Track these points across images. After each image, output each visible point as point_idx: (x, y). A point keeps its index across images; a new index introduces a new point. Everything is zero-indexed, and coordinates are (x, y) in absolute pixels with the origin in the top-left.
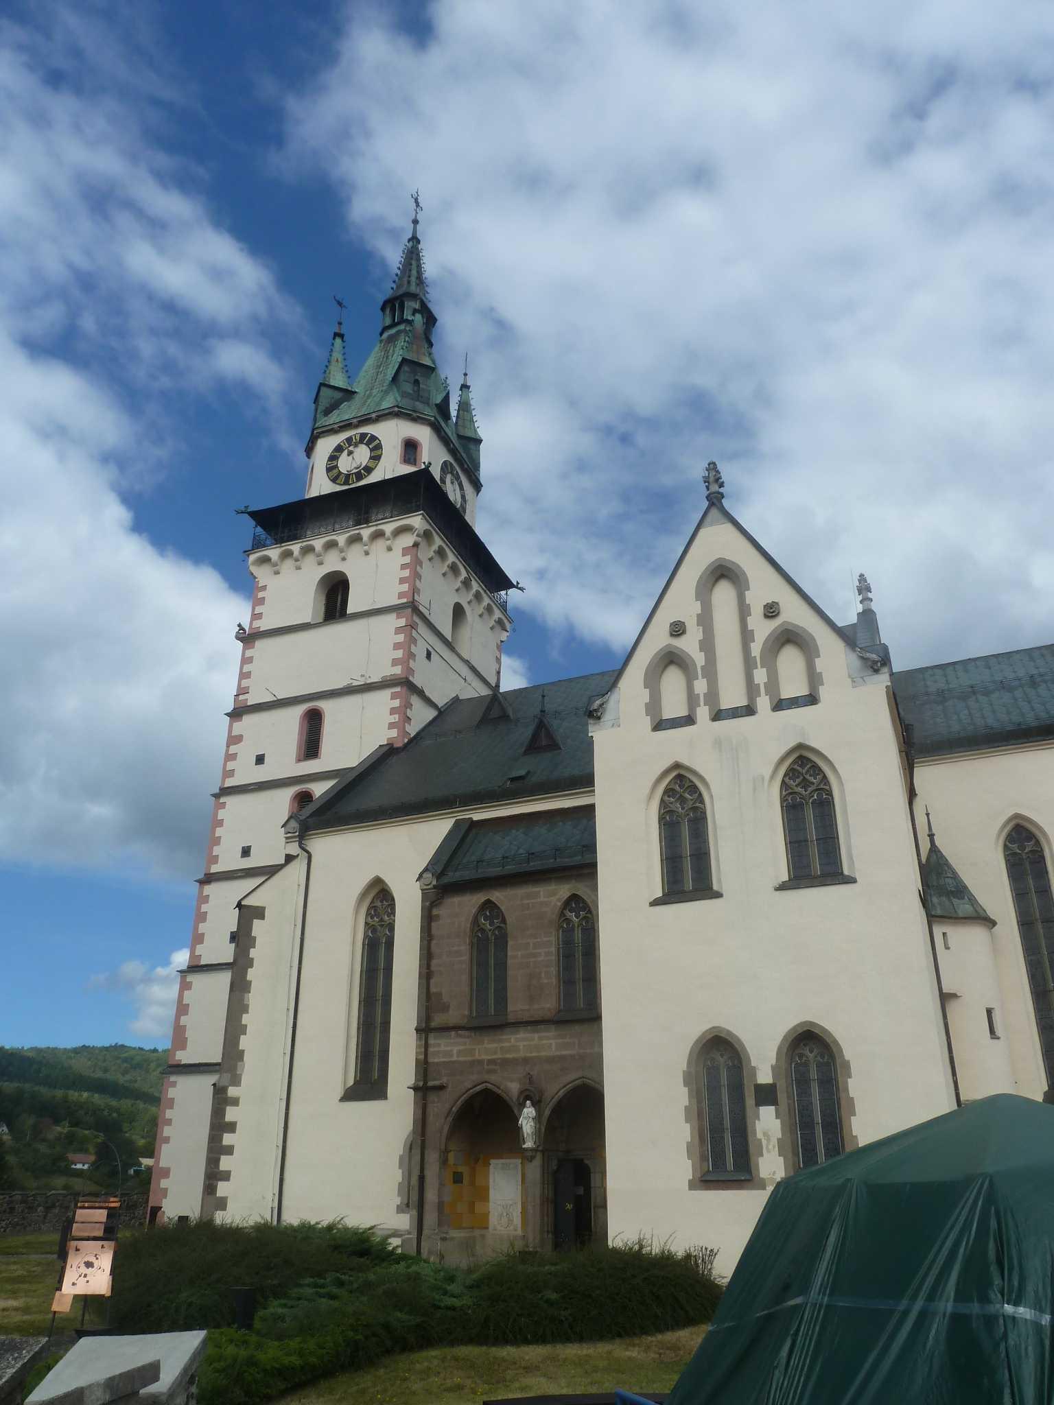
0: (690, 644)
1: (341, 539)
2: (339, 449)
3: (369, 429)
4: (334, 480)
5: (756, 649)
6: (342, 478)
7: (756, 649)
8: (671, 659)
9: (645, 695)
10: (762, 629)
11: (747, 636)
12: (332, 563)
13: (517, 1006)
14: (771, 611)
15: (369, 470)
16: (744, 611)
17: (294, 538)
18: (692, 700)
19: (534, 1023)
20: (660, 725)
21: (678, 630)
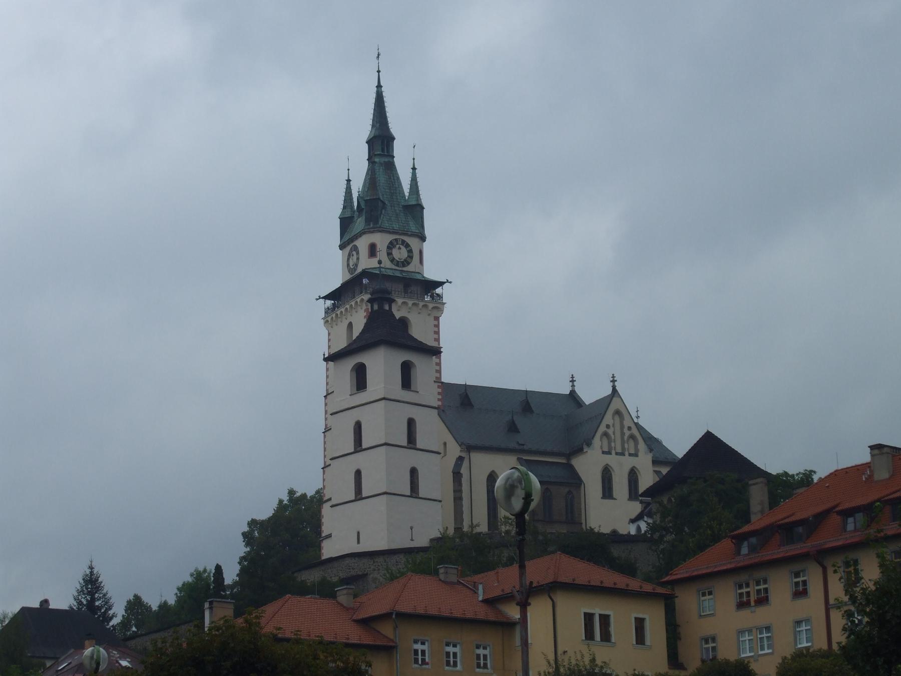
0: (610, 431)
1: (410, 303)
2: (391, 243)
5: (626, 438)
7: (626, 438)
8: (605, 434)
9: (600, 443)
10: (627, 433)
11: (623, 434)
14: (629, 428)
15: (409, 264)
20: (603, 453)
21: (608, 426)
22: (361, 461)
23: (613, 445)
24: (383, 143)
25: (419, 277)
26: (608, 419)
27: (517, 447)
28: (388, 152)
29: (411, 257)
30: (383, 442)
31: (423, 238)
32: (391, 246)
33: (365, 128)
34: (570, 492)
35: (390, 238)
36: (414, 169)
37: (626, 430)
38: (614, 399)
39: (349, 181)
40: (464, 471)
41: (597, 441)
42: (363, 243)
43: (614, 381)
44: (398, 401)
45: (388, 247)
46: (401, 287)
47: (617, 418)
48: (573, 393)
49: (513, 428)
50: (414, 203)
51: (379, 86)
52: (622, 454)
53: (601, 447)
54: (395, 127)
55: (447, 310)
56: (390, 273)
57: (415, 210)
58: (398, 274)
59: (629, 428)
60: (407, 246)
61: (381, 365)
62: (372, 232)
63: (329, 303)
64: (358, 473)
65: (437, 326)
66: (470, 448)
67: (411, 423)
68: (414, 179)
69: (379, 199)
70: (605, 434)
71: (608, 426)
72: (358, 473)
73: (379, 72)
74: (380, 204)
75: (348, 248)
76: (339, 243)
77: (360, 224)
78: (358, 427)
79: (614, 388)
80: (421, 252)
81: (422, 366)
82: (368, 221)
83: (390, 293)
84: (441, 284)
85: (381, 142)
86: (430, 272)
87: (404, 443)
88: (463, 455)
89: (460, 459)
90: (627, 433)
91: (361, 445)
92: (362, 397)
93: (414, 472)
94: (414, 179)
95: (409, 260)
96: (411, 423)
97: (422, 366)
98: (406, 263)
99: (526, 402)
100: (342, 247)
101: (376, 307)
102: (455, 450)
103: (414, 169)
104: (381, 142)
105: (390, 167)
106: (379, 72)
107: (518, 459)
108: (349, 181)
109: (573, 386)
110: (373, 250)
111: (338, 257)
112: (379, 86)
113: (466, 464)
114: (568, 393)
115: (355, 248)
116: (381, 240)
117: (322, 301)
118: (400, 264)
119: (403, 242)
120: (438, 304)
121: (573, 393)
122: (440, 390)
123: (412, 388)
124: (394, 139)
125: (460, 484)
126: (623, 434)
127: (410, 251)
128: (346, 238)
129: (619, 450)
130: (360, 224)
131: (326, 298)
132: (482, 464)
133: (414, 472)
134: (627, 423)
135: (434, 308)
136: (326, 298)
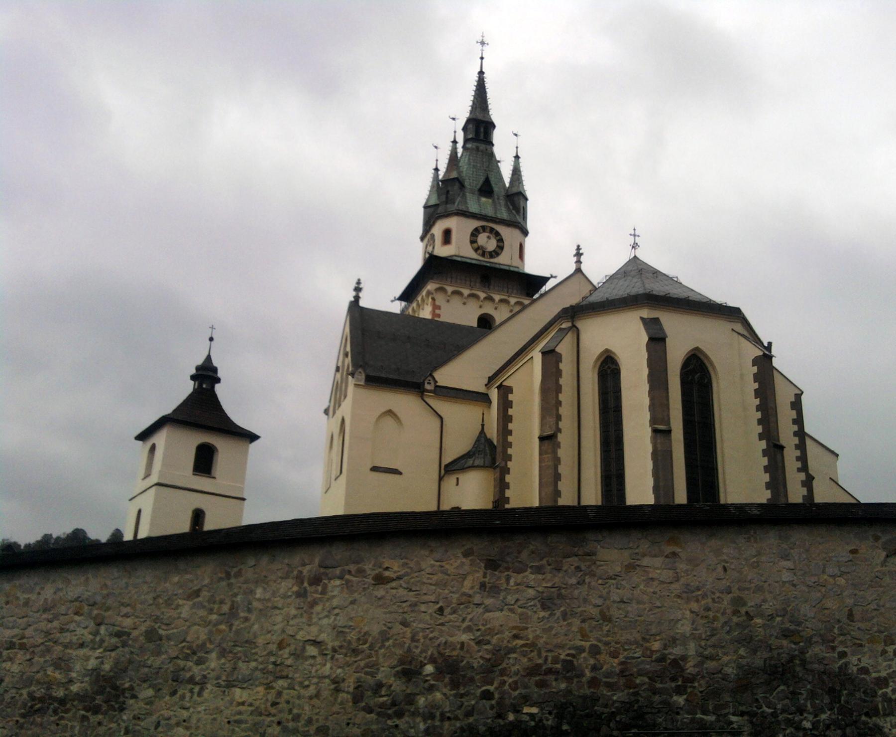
2: (476, 230)
4: (476, 250)
6: (480, 251)
32: (475, 233)
35: (476, 224)
51: (481, 73)
54: (496, 114)
60: (497, 234)
68: (516, 172)
73: (482, 58)
75: (426, 240)
85: (480, 128)
94: (516, 172)
95: (498, 250)
98: (496, 253)
104: (480, 128)
106: (482, 58)
112: (481, 73)
115: (433, 236)
118: (487, 255)
124: (493, 126)
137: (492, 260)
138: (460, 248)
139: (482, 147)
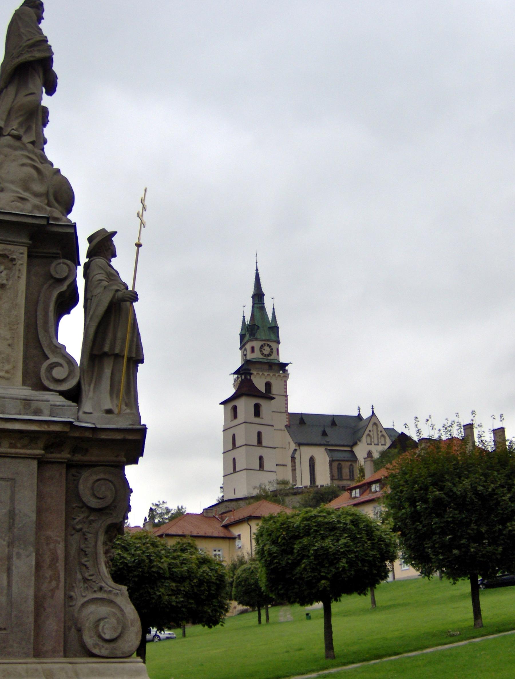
0: (371, 434)
1: (271, 374)
2: (262, 346)
3: (271, 344)
5: (379, 436)
7: (379, 436)
8: (369, 435)
10: (380, 434)
11: (378, 434)
12: (268, 380)
13: (344, 477)
14: (381, 432)
15: (271, 355)
16: (377, 431)
17: (262, 371)
18: (371, 441)
19: (347, 480)
20: (368, 444)
21: (370, 431)
22: (236, 453)
23: (373, 440)
24: (258, 298)
25: (276, 362)
26: (370, 427)
27: (325, 443)
28: (261, 301)
29: (272, 352)
30: (244, 444)
31: (279, 343)
32: (262, 347)
33: (251, 290)
34: (351, 465)
35: (262, 343)
36: (274, 309)
37: (379, 432)
38: (373, 417)
39: (244, 317)
40: (297, 456)
41: (364, 439)
42: (248, 347)
43: (373, 408)
44: (253, 423)
45: (261, 348)
46: (267, 367)
47: (375, 427)
48: (359, 414)
49: (324, 434)
50: (273, 325)
51: (257, 270)
52: (378, 444)
53: (367, 441)
54: (265, 289)
55: (290, 377)
56: (261, 360)
57: (274, 329)
58: (265, 361)
59: (381, 432)
60: (270, 347)
61: (245, 406)
62: (252, 341)
63: (236, 376)
64: (234, 459)
65: (286, 385)
66: (300, 445)
67: (259, 434)
69: (255, 325)
70: (369, 435)
71: (370, 431)
72: (234, 459)
73: (257, 263)
74: (256, 327)
76: (239, 347)
77: (247, 337)
78: (234, 436)
79: (373, 411)
80: (278, 350)
81: (266, 406)
82: (250, 335)
83: (250, 370)
84: (287, 364)
85: (258, 296)
86: (282, 359)
87: (256, 443)
88: (297, 448)
89: (295, 450)
90: (380, 434)
91: (235, 446)
92: (236, 422)
93: (261, 458)
96: (259, 434)
97: (266, 406)
98: (270, 355)
99: (334, 421)
100: (241, 349)
101: (243, 377)
102: (293, 446)
103: (274, 309)
104: (258, 296)
105: (262, 308)
106: (257, 263)
107: (326, 449)
108: (244, 317)
109: (359, 411)
110: (253, 349)
111: (239, 353)
112: (257, 270)
113: (298, 452)
114: (357, 415)
115: (245, 350)
116: (257, 345)
117: (232, 375)
119: (268, 345)
120: (286, 375)
121: (359, 414)
122: (287, 417)
123: (261, 416)
124: (264, 295)
125: (295, 462)
126: (378, 434)
127: (272, 349)
128: (242, 344)
129: (376, 442)
130: (247, 337)
131: (234, 373)
132: (306, 452)
133: (261, 458)
134: (380, 429)
135: (283, 376)
136: (234, 373)
137: (269, 358)
138: (256, 355)
139: (261, 305)
